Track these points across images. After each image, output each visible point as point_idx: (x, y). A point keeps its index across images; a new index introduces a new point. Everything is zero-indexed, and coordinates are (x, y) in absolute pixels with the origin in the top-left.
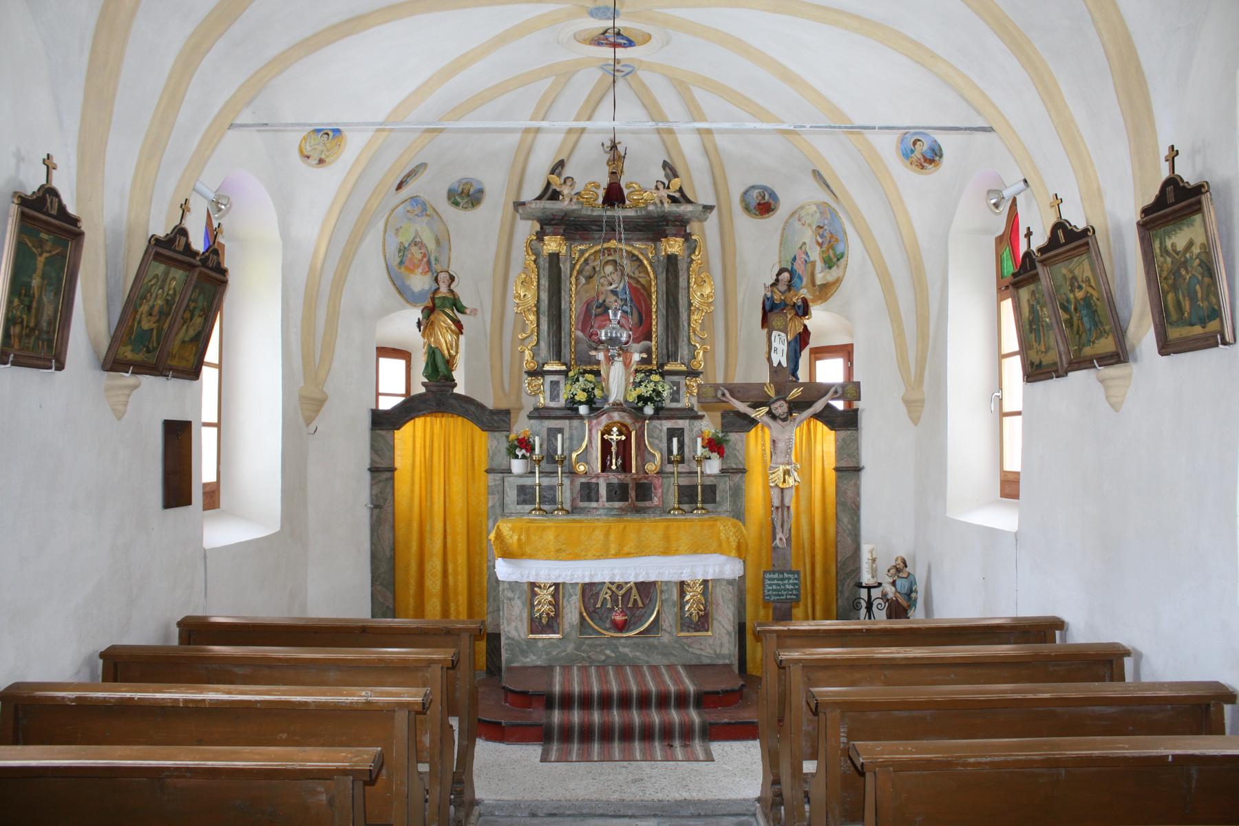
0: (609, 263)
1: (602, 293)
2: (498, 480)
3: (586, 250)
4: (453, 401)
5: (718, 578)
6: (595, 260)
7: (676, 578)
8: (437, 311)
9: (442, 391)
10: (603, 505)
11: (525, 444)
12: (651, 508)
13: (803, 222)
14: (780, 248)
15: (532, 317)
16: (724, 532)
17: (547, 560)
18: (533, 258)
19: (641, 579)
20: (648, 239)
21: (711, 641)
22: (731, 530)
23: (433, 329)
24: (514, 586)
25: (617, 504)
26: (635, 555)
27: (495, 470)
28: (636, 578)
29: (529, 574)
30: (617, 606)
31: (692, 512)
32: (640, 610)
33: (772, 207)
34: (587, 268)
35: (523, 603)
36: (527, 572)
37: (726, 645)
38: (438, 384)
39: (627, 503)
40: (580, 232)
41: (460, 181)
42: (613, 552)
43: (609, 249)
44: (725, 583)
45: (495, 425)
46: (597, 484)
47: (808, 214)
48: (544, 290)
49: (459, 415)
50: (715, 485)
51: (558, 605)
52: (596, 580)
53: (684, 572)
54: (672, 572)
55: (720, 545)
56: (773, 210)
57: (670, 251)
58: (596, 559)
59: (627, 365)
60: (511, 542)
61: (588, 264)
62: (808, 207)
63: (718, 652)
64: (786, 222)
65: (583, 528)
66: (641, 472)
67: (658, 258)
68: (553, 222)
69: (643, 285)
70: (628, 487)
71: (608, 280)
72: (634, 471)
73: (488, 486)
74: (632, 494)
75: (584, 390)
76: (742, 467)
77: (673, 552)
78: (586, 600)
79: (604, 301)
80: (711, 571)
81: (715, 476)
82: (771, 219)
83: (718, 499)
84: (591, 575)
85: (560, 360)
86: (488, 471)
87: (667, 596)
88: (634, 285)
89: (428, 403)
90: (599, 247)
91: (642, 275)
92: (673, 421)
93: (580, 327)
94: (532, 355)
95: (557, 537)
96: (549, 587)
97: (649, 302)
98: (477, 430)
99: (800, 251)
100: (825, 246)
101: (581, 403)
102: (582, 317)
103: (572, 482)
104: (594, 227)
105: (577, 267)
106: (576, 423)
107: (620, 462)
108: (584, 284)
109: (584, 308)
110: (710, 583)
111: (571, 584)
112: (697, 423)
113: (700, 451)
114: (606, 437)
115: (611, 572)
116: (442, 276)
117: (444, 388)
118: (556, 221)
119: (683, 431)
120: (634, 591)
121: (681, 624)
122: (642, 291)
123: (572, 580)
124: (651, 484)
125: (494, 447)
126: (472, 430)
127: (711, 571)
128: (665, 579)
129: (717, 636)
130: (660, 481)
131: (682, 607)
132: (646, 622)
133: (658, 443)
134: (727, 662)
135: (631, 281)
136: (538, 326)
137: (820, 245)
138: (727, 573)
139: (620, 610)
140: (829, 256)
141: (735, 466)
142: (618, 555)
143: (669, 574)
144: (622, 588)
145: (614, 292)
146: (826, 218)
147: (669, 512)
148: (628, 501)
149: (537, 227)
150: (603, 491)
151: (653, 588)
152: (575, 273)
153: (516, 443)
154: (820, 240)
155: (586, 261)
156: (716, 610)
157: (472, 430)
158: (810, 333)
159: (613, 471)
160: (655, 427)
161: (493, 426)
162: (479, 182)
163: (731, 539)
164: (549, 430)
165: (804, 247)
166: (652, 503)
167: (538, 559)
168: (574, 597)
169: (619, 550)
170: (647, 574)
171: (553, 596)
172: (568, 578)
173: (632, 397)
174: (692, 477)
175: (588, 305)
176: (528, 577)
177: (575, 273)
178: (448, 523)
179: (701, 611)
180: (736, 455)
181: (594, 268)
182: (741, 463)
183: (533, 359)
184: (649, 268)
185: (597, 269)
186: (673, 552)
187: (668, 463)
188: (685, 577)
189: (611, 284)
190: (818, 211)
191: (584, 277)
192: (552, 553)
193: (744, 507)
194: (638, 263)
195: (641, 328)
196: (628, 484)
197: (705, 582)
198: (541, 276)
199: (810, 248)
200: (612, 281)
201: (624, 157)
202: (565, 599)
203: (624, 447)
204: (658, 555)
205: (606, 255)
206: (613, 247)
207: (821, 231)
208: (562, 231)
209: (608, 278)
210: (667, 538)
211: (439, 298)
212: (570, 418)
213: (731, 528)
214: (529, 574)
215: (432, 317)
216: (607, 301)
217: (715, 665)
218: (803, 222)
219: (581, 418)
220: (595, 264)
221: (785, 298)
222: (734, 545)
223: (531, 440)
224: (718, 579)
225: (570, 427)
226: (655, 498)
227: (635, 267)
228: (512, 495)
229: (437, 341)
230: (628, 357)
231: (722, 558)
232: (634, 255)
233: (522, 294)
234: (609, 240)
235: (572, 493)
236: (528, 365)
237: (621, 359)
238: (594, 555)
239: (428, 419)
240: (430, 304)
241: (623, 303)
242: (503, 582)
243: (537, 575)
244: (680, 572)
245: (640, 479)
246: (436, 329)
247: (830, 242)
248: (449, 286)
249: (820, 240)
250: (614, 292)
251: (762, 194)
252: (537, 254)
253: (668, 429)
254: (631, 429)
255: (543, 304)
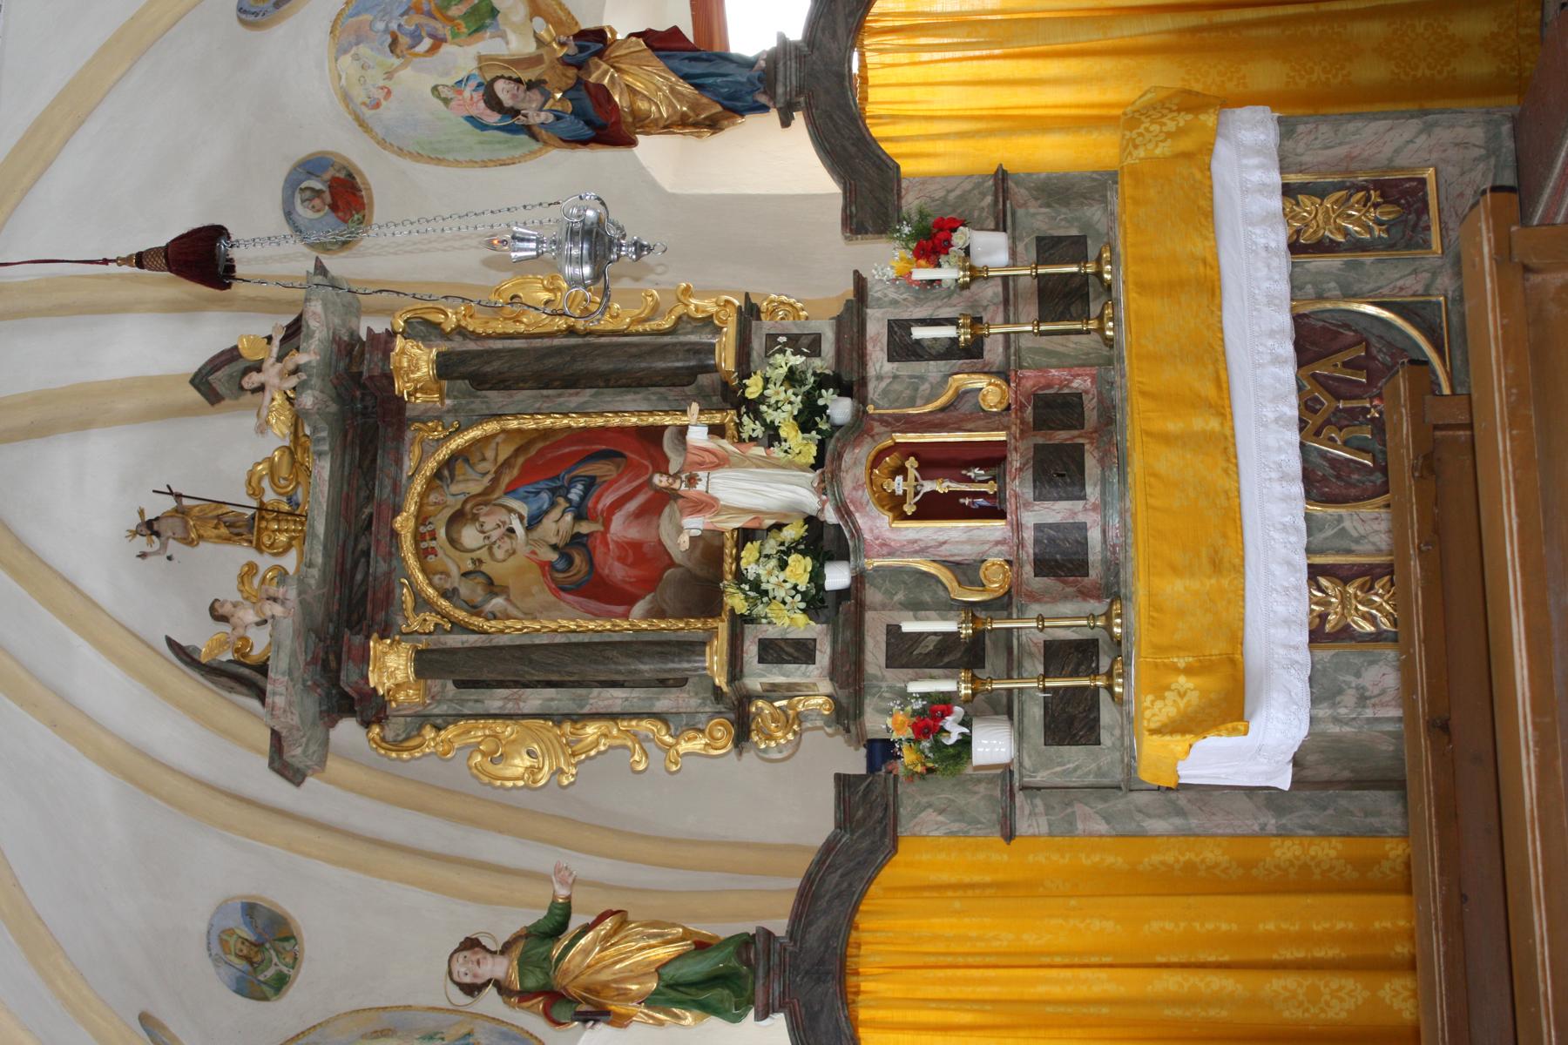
0: (455, 536)
1: (534, 553)
2: (1034, 806)
3: (417, 595)
4: (813, 938)
5: (1277, 158)
6: (447, 574)
7: (1282, 262)
8: (560, 982)
9: (782, 963)
10: (1095, 508)
11: (930, 716)
12: (1100, 393)
13: (380, 95)
14: (448, 163)
15: (592, 730)
16: (1150, 146)
17: (1243, 597)
18: (429, 733)
19: (1288, 350)
20: (399, 437)
21: (1450, 171)
22: (1147, 130)
23: (606, 985)
24: (1322, 689)
25: (1091, 463)
26: (1221, 366)
27: (1005, 815)
28: (1286, 362)
29: (1287, 647)
30: (1367, 411)
31: (1109, 288)
32: (1374, 351)
33: (342, 175)
34: (464, 591)
35: (1372, 663)
36: (1282, 651)
37: (1460, 132)
38: (761, 972)
39: (1087, 447)
40: (369, 607)
41: (216, 960)
42: (1214, 424)
43: (418, 537)
44: (1289, 144)
45: (878, 814)
46: (1038, 527)
47: (362, 80)
48: (517, 700)
49: (851, 925)
50: (1039, 240)
51: (1372, 567)
52: (1295, 465)
53: (1263, 241)
54: (1264, 272)
55: (1187, 156)
56: (350, 175)
57: (425, 370)
58: (1237, 465)
59: (721, 462)
60: (1196, 694)
61: (455, 590)
62: (343, 81)
63: (1483, 152)
64: (383, 143)
65: (1151, 501)
66: (1005, 420)
67: (448, 411)
68: (333, 664)
69: (518, 452)
70: (1043, 446)
71: (501, 538)
72: (1000, 436)
73: (1051, 835)
74: (1061, 436)
75: (783, 565)
76: (991, 182)
77: (1209, 272)
78: (1353, 492)
79: (554, 547)
80: (1257, 177)
81: (1014, 241)
82: (372, 181)
83: (1074, 232)
84: (1282, 478)
85: (704, 644)
86: (1009, 835)
87: (1333, 285)
88: (515, 472)
89: (817, 1008)
90: (412, 561)
91: (490, 454)
92: (869, 347)
93: (620, 609)
94: (692, 734)
95: (1175, 570)
96: (1320, 589)
97: (561, 436)
98: (890, 874)
99: (453, 104)
100: (444, 30)
101: (817, 577)
102: (593, 604)
103: (1034, 597)
104: (359, 577)
105: (461, 615)
106: (872, 595)
107: (976, 472)
108: (508, 599)
109: (570, 597)
110: (1294, 178)
111: (1310, 532)
112: (874, 291)
113: (948, 273)
114: (909, 509)
115: (1274, 426)
116: (463, 970)
117: (775, 959)
118: (331, 657)
119: (896, 321)
120: (1321, 370)
121: (1408, 247)
122: (533, 452)
123: (1297, 530)
124: (1035, 395)
125: (940, 818)
126: (892, 890)
127: (1257, 177)
128: (1284, 288)
129: (1435, 156)
130: (1028, 373)
131: (1358, 246)
132: (1409, 337)
133: (927, 386)
134: (1506, 128)
135: (506, 480)
136: (613, 717)
137: (438, 41)
138: (1262, 137)
139: (1376, 402)
140: (466, 16)
141: (989, 199)
142: (1222, 408)
143: (1270, 279)
144: (1316, 400)
145: (533, 523)
146: (371, 24)
147: (1109, 343)
148: (1083, 445)
149: (347, 730)
150: (1056, 512)
151: (1313, 322)
152: (478, 621)
153: (926, 744)
154: (427, 43)
155: (444, 594)
156: (1367, 160)
157: (892, 890)
158: (651, 30)
159: (1002, 489)
160: (885, 393)
161: (880, 821)
162: (221, 909)
163: (1171, 126)
164: (891, 662)
165: (445, 93)
166: (1087, 392)
167: (1243, 620)
168: (1347, 524)
169: (1210, 406)
170: (1272, 334)
171: (1346, 581)
172: (1293, 539)
173: (801, 445)
174: (1015, 295)
175: (561, 588)
176: (1296, 648)
177: (478, 621)
178: (1160, 959)
179: (1368, 199)
180: (960, 197)
181: (465, 575)
182: (978, 185)
183: (702, 731)
184: (475, 433)
185: (470, 566)
186: (1209, 272)
187: (980, 355)
188: (1278, 238)
189: (511, 531)
190: (354, 50)
191: (487, 601)
192: (1225, 582)
193: (1093, 172)
194: (460, 466)
195: (627, 453)
196: (1036, 447)
197: (1288, 191)
198: (479, 709)
199: (447, 74)
200: (503, 530)
201: (179, 496)
202: (1354, 547)
203: (933, 461)
204: (1220, 308)
205: (433, 544)
206: (412, 523)
207: (404, 40)
208: (357, 640)
209: (493, 539)
210: (1172, 288)
211: (522, 975)
212: (861, 607)
213: (1141, 130)
214: (1287, 647)
215: (574, 991)
216: (554, 540)
217: (1517, 159)
218: (380, 95)
219: (859, 578)
220: (454, 572)
221: (560, 90)
222: (1184, 119)
223: (918, 705)
224: (1280, 161)
225: (884, 607)
226: (1075, 385)
227: (470, 470)
228: (1074, 761)
229: (637, 975)
230: (697, 459)
231: (1223, 150)
232: (438, 475)
233: (528, 762)
234: (395, 535)
235: (1066, 598)
236: (719, 744)
237: (702, 474)
238: (1226, 471)
239: (863, 1014)
240: (539, 1003)
241: (561, 500)
242: (1313, 720)
243: (1287, 622)
244: (1264, 254)
245: (1023, 422)
246: (605, 976)
247: (430, 15)
248: (493, 953)
249: (427, 43)
250: (533, 523)
251: (308, 194)
252: (422, 719)
253: (889, 361)
254: (889, 442)
255: (554, 704)
